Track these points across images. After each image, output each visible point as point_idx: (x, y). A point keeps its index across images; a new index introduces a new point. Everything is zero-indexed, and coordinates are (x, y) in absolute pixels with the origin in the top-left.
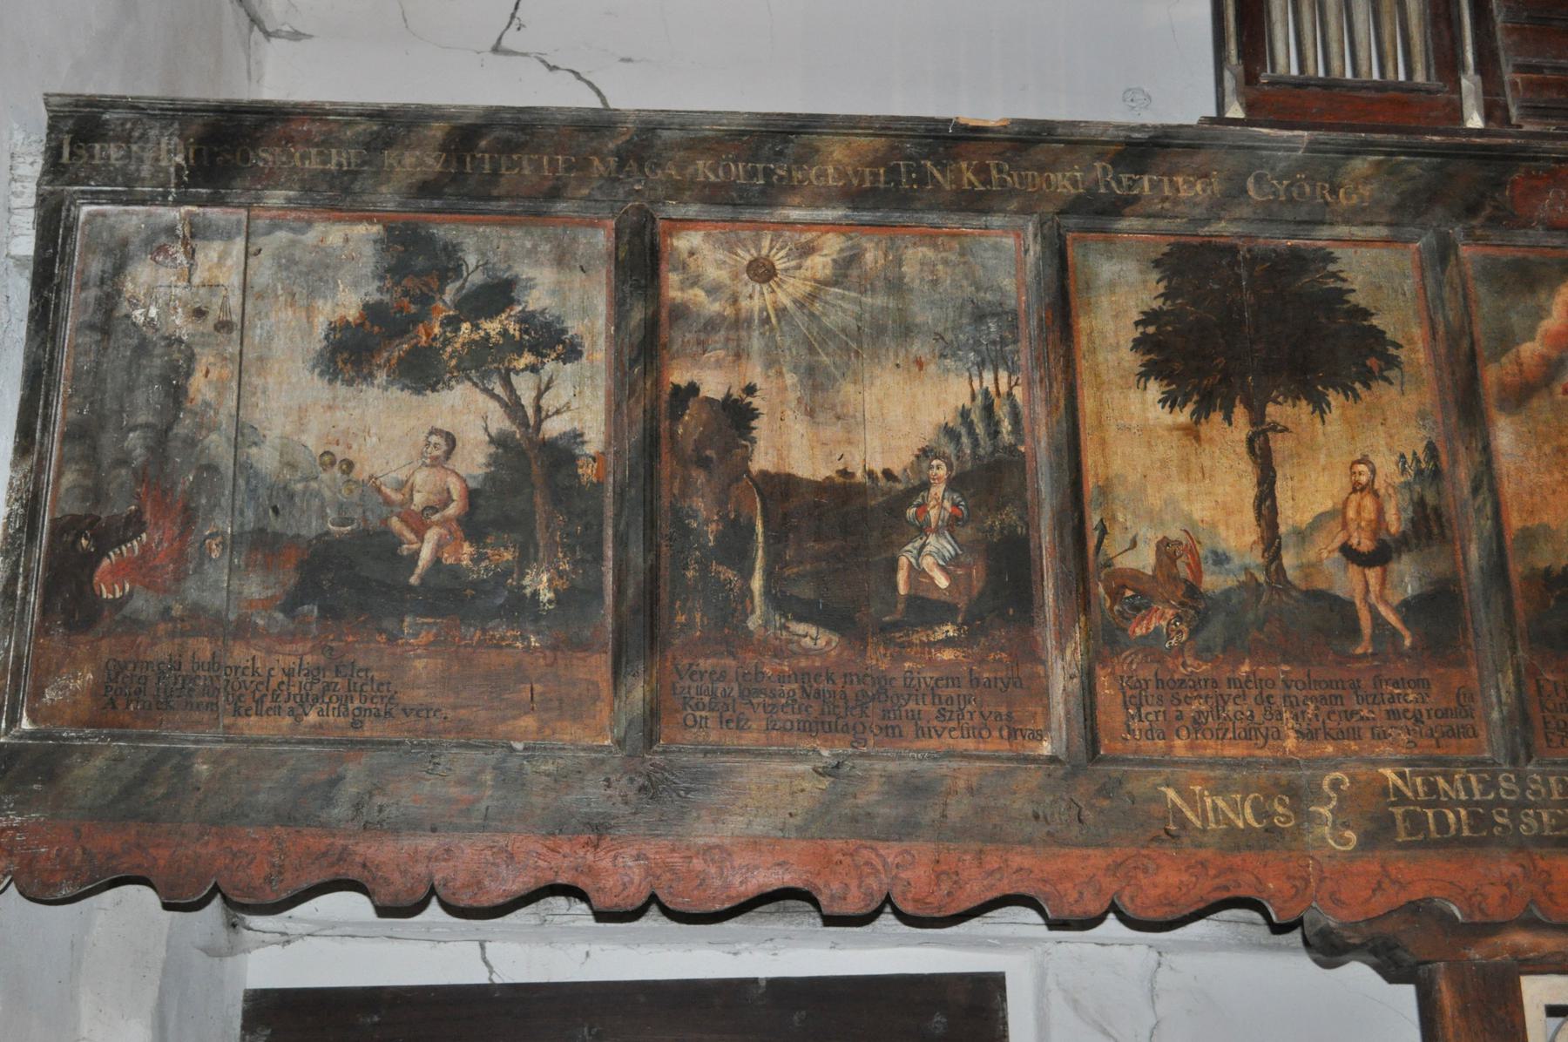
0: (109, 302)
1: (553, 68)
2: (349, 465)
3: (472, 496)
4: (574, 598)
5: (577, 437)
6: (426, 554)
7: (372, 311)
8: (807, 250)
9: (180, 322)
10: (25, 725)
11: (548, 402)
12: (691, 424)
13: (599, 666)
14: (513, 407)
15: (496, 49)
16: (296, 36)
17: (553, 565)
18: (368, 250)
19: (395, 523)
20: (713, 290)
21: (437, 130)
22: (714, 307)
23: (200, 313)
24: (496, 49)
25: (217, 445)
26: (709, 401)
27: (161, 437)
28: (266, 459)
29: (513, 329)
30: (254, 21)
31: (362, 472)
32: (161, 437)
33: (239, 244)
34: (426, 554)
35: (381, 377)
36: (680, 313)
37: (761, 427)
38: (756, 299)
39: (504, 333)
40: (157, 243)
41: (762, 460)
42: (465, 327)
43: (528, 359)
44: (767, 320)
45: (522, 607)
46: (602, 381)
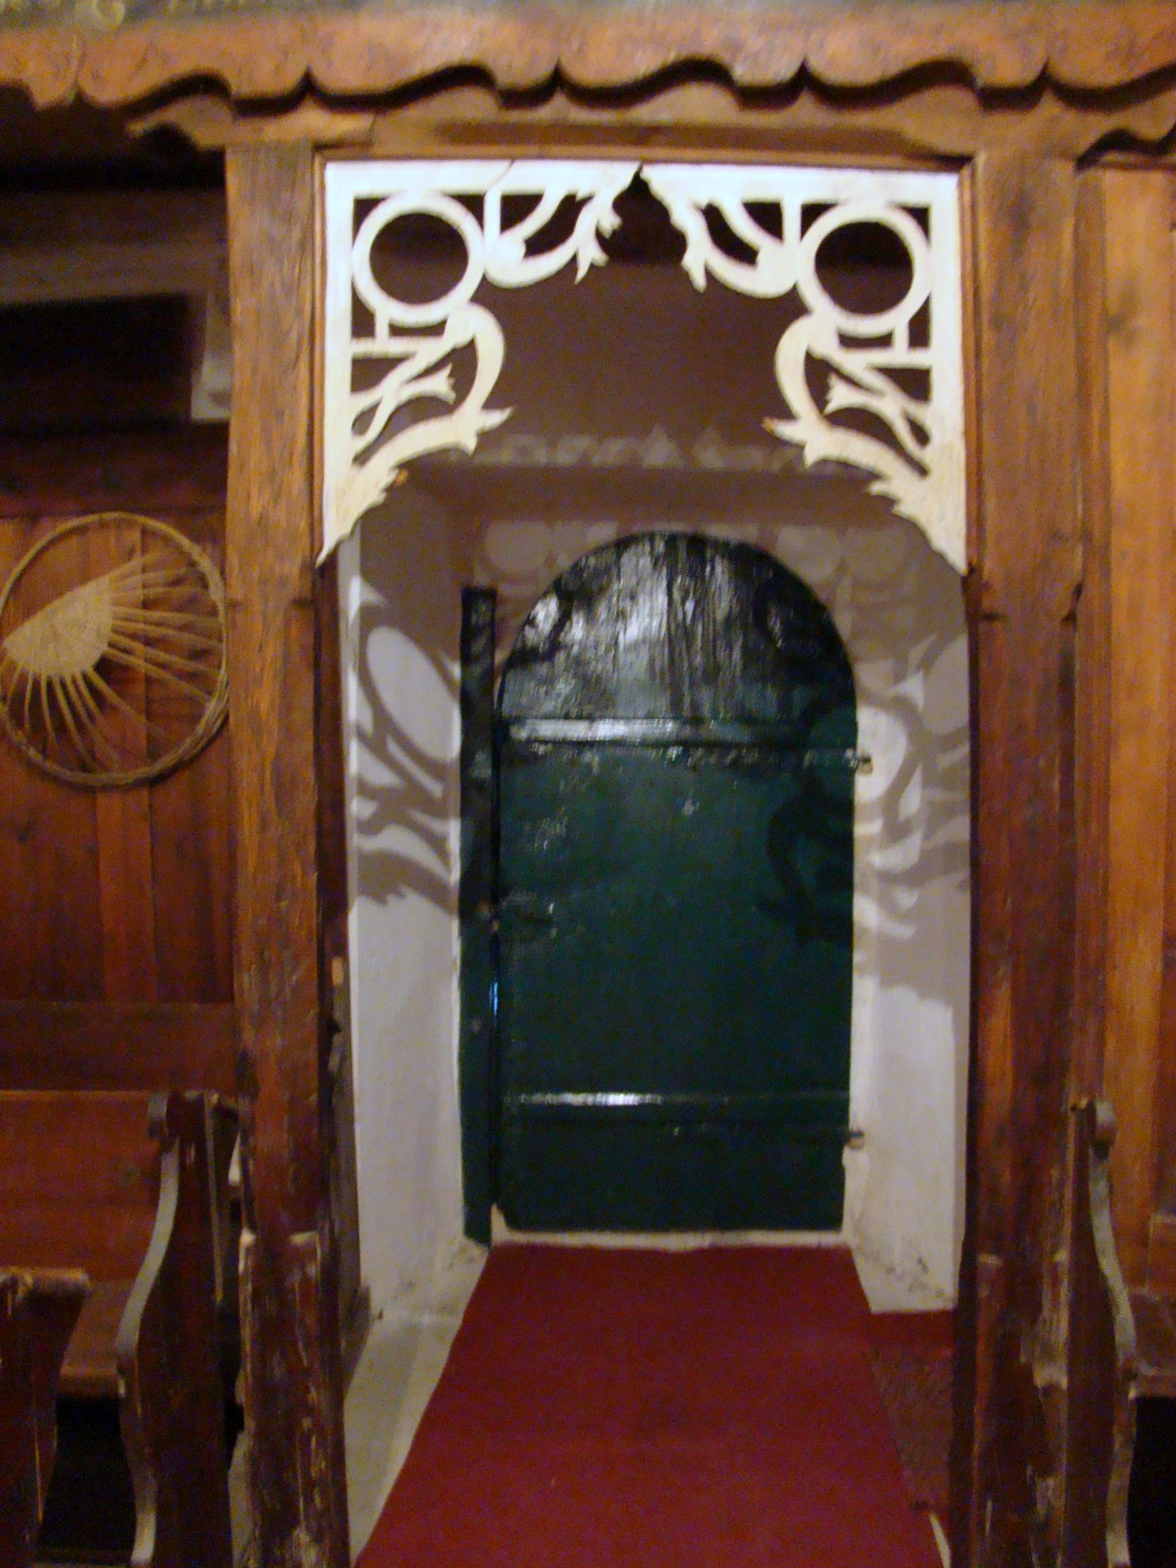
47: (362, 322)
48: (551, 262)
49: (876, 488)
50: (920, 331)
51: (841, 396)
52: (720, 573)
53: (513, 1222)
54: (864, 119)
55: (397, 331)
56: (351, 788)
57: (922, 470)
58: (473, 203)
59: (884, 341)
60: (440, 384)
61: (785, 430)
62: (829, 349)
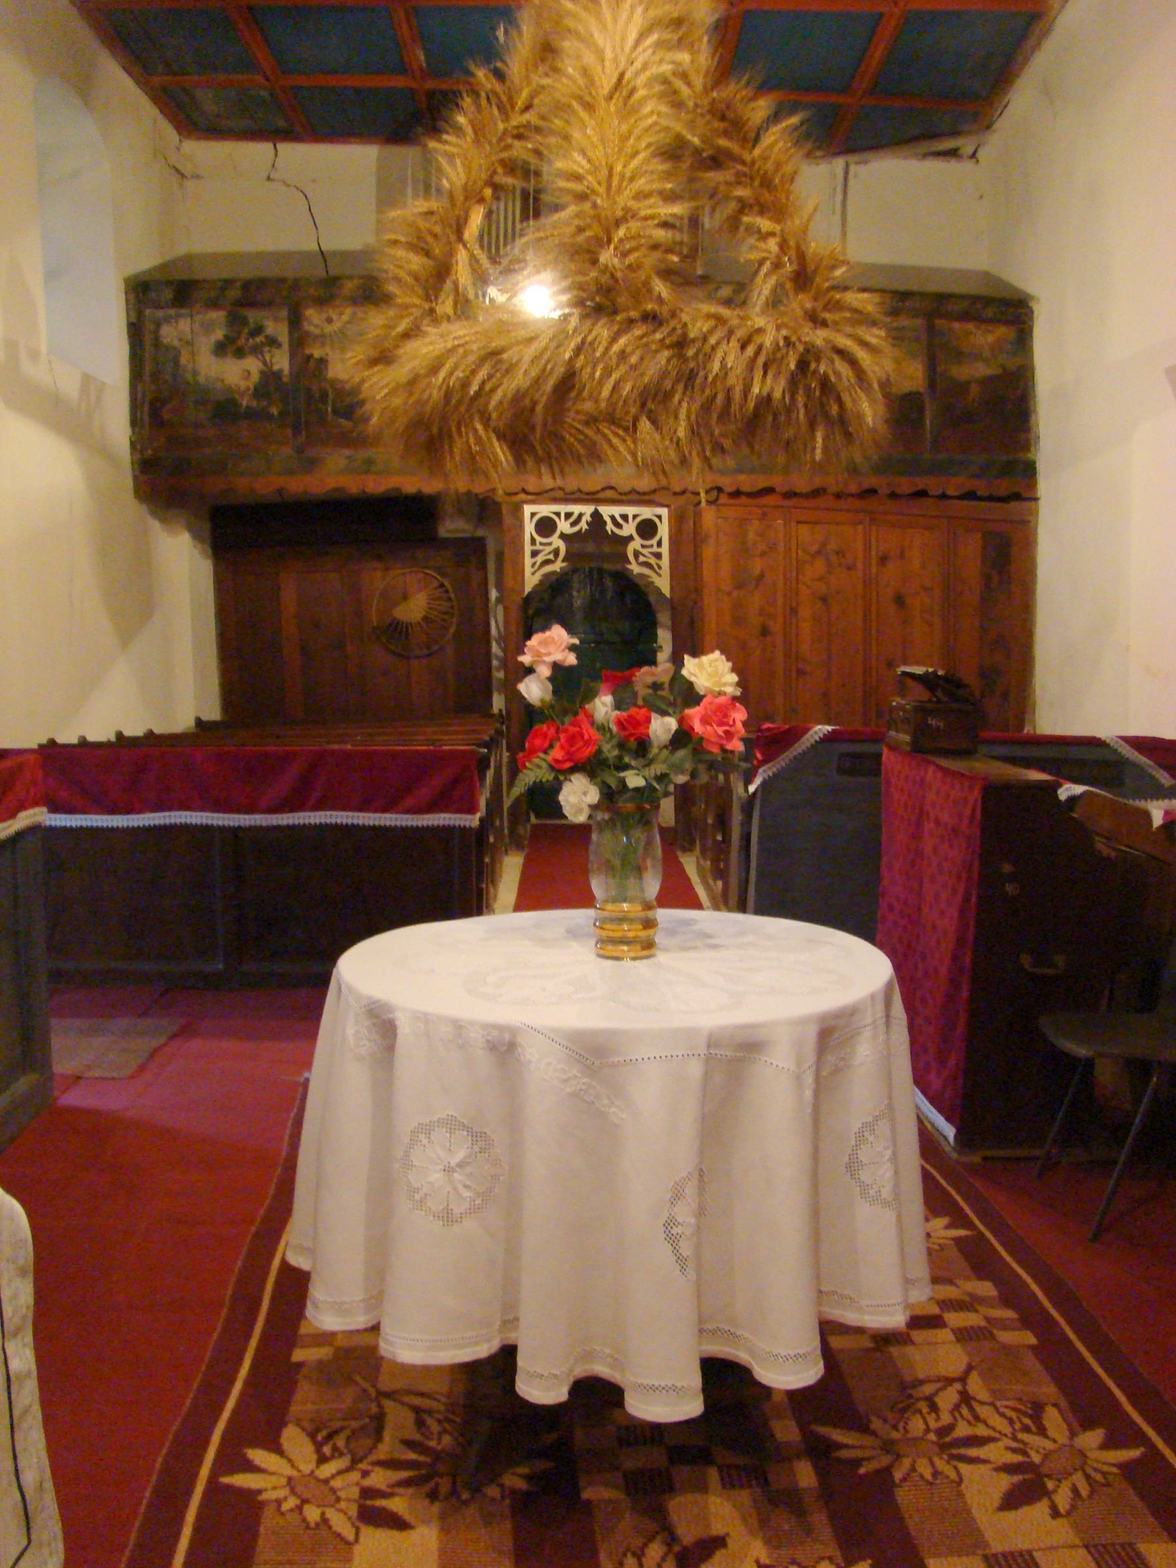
0: (157, 338)
1: (288, 186)
2: (223, 381)
3: (256, 389)
4: (283, 414)
5: (281, 371)
6: (244, 403)
7: (226, 337)
8: (342, 314)
9: (176, 343)
10: (150, 452)
11: (274, 360)
12: (312, 364)
13: (289, 432)
14: (265, 363)
15: (269, 179)
16: (197, 177)
17: (277, 406)
18: (223, 319)
19: (236, 396)
20: (316, 326)
21: (238, 284)
22: (317, 331)
23: (180, 340)
24: (269, 179)
25: (189, 377)
26: (317, 359)
27: (175, 376)
28: (201, 380)
29: (263, 339)
30: (183, 176)
31: (226, 382)
32: (175, 376)
33: (189, 319)
34: (244, 403)
35: (230, 355)
36: (308, 334)
37: (330, 367)
38: (328, 329)
39: (262, 342)
40: (168, 320)
41: (331, 374)
42: (251, 340)
43: (267, 348)
44: (331, 336)
45: (270, 417)
46: (288, 355)
47: (533, 542)
48: (576, 529)
49: (650, 580)
50: (659, 544)
51: (642, 559)
52: (609, 583)
53: (537, 817)
54: (646, 497)
55: (541, 544)
56: (493, 657)
57: (659, 575)
58: (558, 514)
59: (652, 546)
60: (551, 557)
61: (629, 567)
62: (639, 548)
